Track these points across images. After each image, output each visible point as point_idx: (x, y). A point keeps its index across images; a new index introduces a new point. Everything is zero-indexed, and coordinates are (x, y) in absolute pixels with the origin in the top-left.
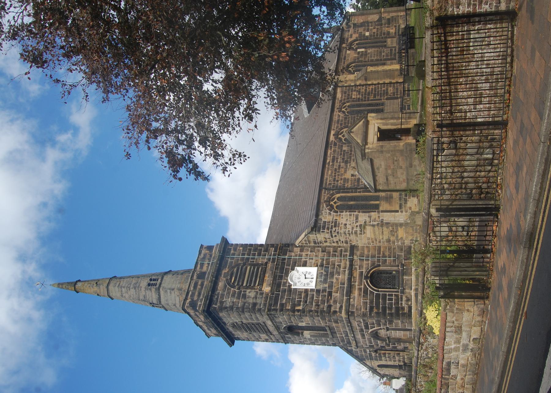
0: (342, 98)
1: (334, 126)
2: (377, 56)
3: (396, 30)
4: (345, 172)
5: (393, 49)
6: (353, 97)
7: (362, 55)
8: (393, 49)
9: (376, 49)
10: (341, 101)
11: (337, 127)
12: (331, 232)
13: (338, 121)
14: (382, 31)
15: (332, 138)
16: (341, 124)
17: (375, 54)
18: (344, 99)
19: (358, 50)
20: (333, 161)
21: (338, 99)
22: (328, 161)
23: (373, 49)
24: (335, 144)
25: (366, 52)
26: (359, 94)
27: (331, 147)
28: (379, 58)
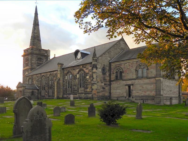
0: (54, 74)
1: (46, 74)
2: (74, 84)
3: (89, 92)
4: (35, 81)
5: (77, 91)
6: (54, 78)
7: (75, 77)
8: (77, 91)
9: (77, 83)
10: (53, 74)
11: (45, 75)
12: (84, 73)
13: (47, 75)
14: (88, 84)
15: (42, 74)
16: (46, 76)
17: (75, 83)
18: (53, 75)
19: (78, 75)
20: (38, 77)
21: (54, 73)
22: (37, 75)
23: (78, 82)
24: (41, 76)
25: (77, 79)
26: (55, 80)
27: (40, 75)
28: (73, 85)
